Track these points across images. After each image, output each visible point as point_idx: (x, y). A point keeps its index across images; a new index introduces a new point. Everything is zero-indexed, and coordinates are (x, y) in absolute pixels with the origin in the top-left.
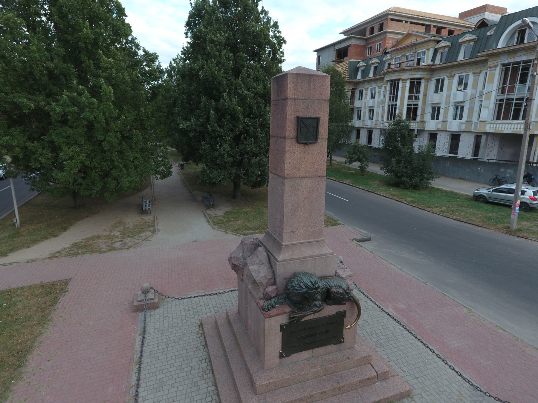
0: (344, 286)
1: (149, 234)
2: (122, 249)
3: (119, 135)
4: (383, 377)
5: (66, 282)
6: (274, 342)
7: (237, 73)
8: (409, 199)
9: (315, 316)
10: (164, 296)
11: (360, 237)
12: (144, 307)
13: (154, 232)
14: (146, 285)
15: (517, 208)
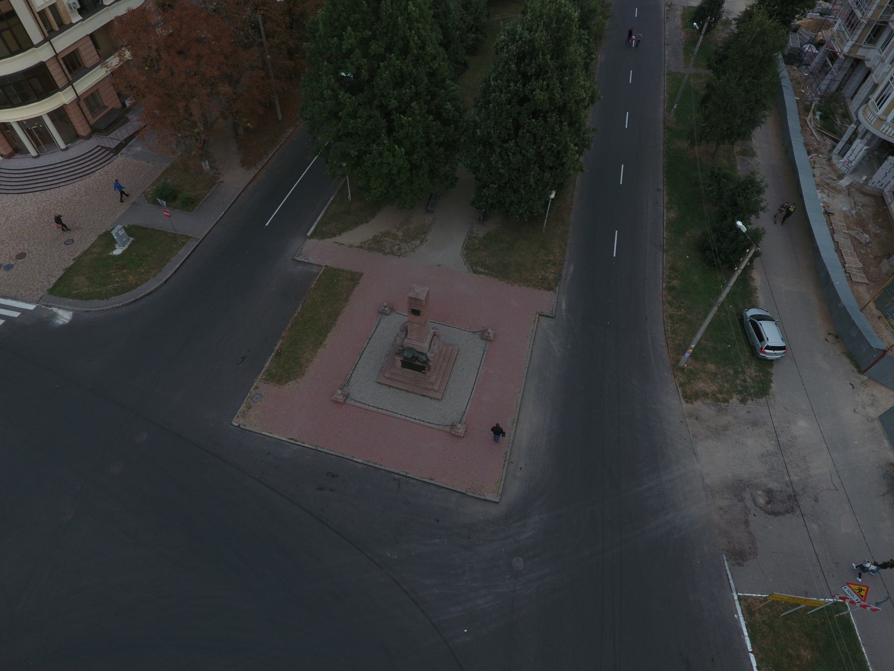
0: (424, 359)
1: (418, 242)
2: (395, 255)
3: (408, 174)
4: (435, 391)
5: (361, 275)
6: (399, 364)
7: (518, 126)
8: (675, 283)
9: (414, 363)
10: (392, 310)
11: (547, 312)
12: (383, 313)
13: (422, 242)
14: (385, 304)
15: (687, 355)
